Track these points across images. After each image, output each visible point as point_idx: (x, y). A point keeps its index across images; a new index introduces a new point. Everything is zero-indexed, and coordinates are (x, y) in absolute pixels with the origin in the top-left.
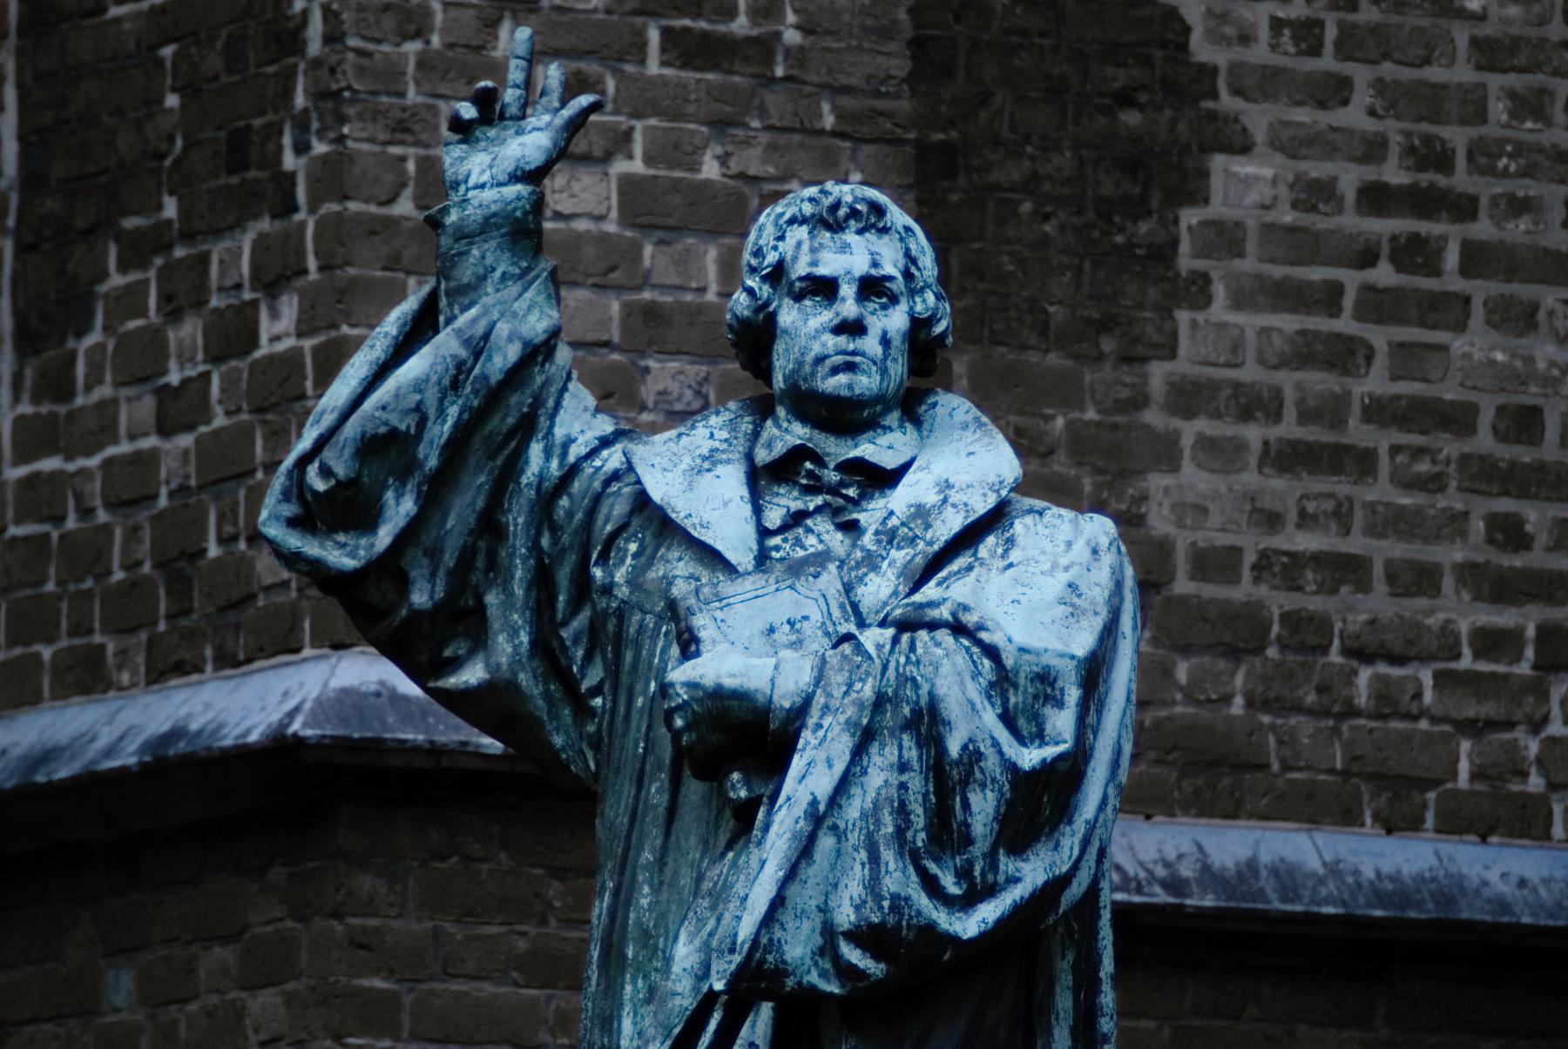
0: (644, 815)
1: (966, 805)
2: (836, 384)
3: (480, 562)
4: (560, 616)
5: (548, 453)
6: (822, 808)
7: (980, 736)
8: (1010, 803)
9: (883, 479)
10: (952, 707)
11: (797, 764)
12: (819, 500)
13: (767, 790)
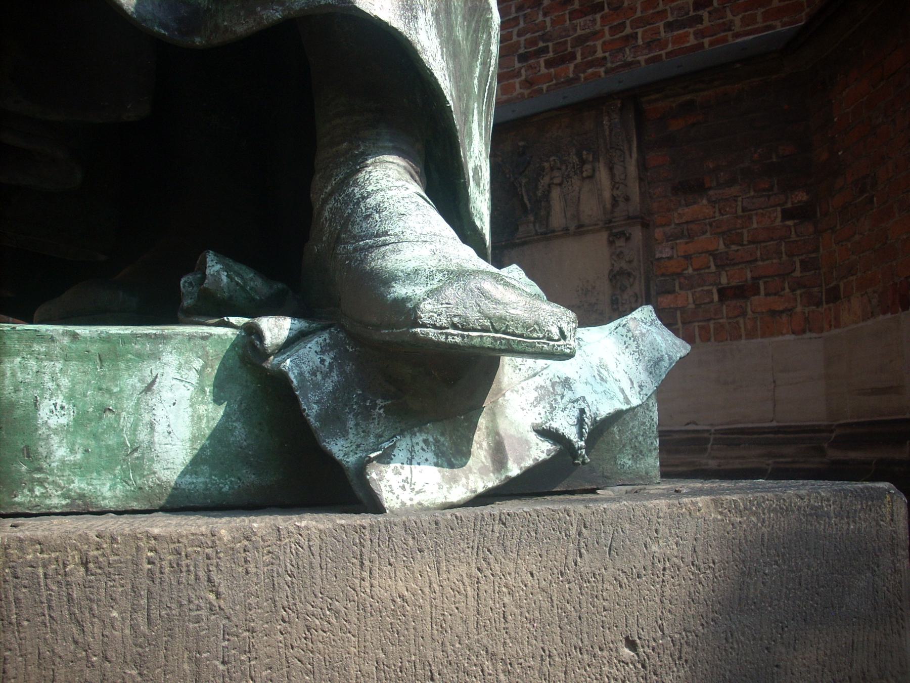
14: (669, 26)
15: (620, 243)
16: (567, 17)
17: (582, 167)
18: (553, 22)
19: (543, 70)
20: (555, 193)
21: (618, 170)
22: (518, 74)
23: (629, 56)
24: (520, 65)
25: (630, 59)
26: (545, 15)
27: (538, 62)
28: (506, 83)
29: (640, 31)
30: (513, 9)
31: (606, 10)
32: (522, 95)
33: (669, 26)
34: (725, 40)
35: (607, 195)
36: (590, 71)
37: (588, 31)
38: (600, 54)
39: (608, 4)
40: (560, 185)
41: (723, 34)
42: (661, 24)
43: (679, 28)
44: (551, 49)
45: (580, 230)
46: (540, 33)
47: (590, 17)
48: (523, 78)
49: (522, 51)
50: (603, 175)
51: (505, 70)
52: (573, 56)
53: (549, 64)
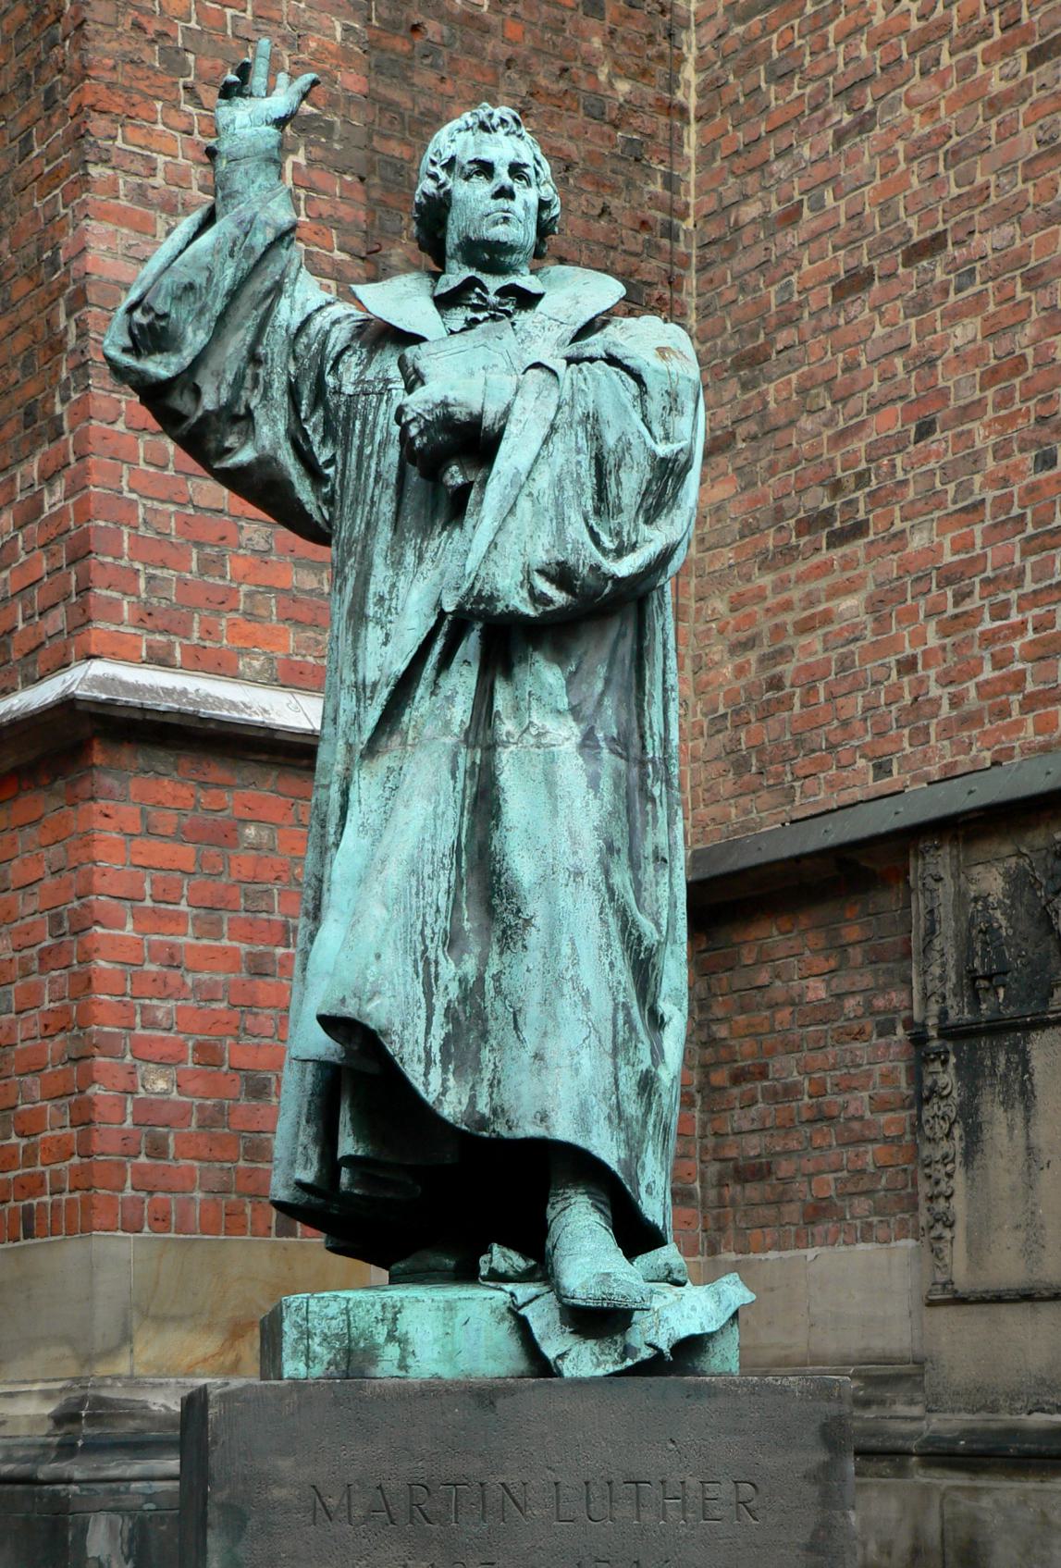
0: (377, 520)
1: (619, 483)
2: (500, 233)
3: (248, 383)
4: (303, 415)
5: (292, 309)
6: (523, 478)
7: (629, 429)
8: (650, 482)
9: (527, 300)
10: (607, 412)
11: (504, 448)
12: (486, 314)
13: (475, 476)
28: (1042, 711)
51: (1041, 687)
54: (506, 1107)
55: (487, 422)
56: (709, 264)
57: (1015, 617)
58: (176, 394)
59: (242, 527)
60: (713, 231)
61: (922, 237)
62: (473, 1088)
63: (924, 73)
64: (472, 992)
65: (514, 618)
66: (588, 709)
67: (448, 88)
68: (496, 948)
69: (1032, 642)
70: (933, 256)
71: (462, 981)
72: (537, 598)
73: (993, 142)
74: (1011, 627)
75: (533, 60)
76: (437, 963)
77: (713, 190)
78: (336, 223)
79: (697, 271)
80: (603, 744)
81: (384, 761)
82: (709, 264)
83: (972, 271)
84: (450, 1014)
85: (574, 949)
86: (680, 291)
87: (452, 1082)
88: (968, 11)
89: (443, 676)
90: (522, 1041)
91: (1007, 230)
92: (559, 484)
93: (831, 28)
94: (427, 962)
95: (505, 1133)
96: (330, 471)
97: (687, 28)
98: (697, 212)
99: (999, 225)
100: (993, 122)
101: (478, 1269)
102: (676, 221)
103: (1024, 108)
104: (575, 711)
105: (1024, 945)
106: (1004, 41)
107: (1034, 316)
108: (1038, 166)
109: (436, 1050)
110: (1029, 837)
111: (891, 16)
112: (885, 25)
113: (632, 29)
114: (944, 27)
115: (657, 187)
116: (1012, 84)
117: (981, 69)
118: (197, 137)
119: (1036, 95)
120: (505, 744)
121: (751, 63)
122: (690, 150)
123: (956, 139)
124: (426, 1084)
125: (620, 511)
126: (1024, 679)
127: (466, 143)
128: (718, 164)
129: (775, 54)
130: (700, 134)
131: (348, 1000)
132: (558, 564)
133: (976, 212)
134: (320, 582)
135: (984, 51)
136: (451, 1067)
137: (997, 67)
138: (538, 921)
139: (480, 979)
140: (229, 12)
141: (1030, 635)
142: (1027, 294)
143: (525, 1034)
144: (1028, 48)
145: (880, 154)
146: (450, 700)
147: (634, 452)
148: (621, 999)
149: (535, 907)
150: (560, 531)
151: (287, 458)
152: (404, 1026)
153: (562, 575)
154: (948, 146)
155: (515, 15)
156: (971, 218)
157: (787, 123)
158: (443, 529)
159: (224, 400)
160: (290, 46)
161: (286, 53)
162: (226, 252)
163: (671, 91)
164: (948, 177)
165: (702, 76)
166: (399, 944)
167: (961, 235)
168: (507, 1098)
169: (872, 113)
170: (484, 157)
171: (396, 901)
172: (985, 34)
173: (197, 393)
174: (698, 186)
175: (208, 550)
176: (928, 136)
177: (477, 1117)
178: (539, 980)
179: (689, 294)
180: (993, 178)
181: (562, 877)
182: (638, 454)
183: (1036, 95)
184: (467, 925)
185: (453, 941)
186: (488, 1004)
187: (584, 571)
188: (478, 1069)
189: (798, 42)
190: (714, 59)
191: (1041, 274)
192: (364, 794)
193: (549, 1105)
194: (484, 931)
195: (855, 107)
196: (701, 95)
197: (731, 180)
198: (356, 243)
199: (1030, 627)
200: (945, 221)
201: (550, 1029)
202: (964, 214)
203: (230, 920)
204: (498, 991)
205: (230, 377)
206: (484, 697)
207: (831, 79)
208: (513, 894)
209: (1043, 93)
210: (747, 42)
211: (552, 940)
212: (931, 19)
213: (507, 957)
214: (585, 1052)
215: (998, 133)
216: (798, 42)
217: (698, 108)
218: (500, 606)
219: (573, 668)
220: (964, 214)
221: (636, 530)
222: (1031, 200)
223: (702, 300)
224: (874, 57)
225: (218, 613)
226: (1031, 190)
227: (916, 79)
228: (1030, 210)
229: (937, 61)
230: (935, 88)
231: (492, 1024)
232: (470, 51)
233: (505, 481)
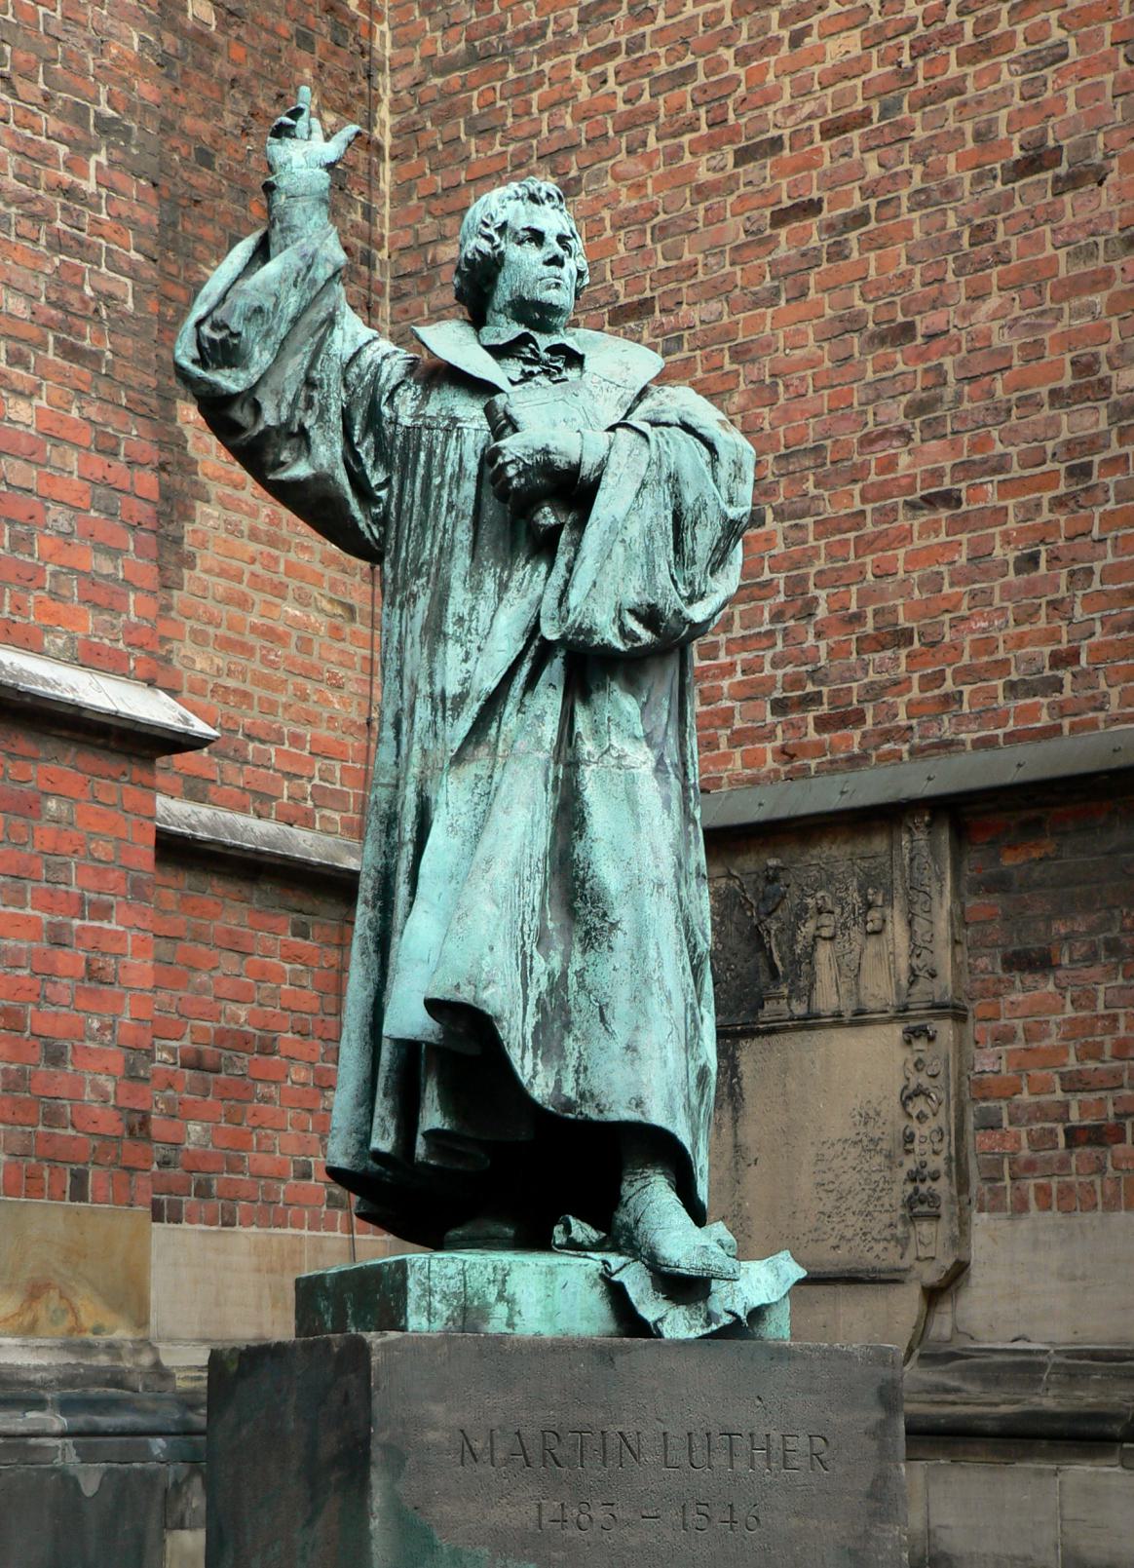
1: (694, 538)
4: (356, 440)
8: (719, 540)
10: (687, 474)
11: (601, 497)
14: (1012, 688)
15: (920, 1044)
16: (854, 647)
17: (866, 913)
18: (831, 651)
19: (812, 735)
20: (824, 952)
21: (921, 924)
22: (771, 736)
23: (946, 729)
24: (775, 719)
25: (948, 736)
26: (818, 635)
27: (804, 719)
28: (750, 747)
29: (967, 689)
30: (766, 615)
31: (916, 644)
32: (776, 771)
33: (1012, 688)
34: (1093, 725)
35: (903, 963)
36: (887, 747)
37: (886, 676)
38: (902, 720)
39: (921, 635)
40: (832, 938)
41: (1091, 715)
42: (999, 683)
43: (1027, 695)
44: (825, 700)
45: (860, 1018)
46: (809, 668)
47: (889, 653)
48: (779, 743)
49: (777, 694)
50: (897, 929)
51: (749, 725)
52: (859, 718)
53: (822, 724)
54: (596, 1092)
55: (585, 471)
56: (404, 295)
57: (723, 659)
58: (237, 407)
59: (48, 508)
60: (408, 264)
61: (629, 300)
62: (558, 1073)
63: (630, 152)
64: (558, 985)
65: (607, 650)
66: (658, 738)
67: (180, 98)
68: (578, 947)
69: (740, 683)
70: (639, 319)
71: (551, 975)
72: (625, 634)
73: (700, 224)
74: (719, 667)
75: (254, 83)
76: (532, 957)
77: (409, 226)
78: (133, 224)
79: (391, 300)
80: (670, 769)
81: (470, 770)
82: (404, 295)
83: (680, 338)
84: (540, 1006)
85: (659, 953)
86: (376, 317)
87: (540, 1067)
88: (675, 104)
89: (528, 696)
90: (612, 1034)
91: (715, 306)
92: (649, 534)
93: (535, 96)
94: (524, 955)
95: (594, 1115)
96: (383, 494)
97: (383, 71)
98: (391, 244)
99: (707, 301)
100: (701, 206)
101: (551, 1235)
102: (374, 251)
103: (731, 199)
104: (648, 738)
105: (733, 959)
106: (711, 137)
107: (742, 387)
108: (746, 252)
109: (529, 1036)
110: (740, 861)
111: (596, 95)
112: (590, 102)
113: (336, 65)
114: (651, 114)
115: (357, 217)
116: (719, 175)
117: (688, 158)
118: (12, 126)
119: (742, 190)
120: (588, 763)
121: (449, 114)
122: (386, 185)
123: (662, 217)
124: (522, 1068)
125: (694, 563)
126: (733, 717)
127: (517, 211)
128: (414, 202)
129: (476, 111)
130: (395, 172)
131: (462, 987)
132: (649, 606)
133: (684, 285)
134: (116, 568)
135: (691, 142)
136: (540, 1052)
137: (704, 158)
138: (624, 926)
139: (564, 974)
140: (41, 10)
141: (739, 677)
142: (735, 367)
143: (614, 1027)
144: (735, 147)
145: (585, 218)
146: (540, 718)
147: (709, 512)
148: (689, 1000)
149: (621, 912)
150: (651, 577)
151: (342, 477)
152: (511, 1013)
153: (650, 616)
154: (655, 221)
155: (238, 38)
156: (680, 289)
157: (488, 176)
158: (527, 562)
159: (284, 418)
160: (95, 50)
161: (91, 56)
162: (291, 281)
163: (369, 128)
164: (655, 250)
165: (398, 118)
166: (507, 938)
167: (669, 304)
168: (596, 1083)
169: (578, 180)
170: (536, 226)
171: (505, 899)
172: (692, 126)
173: (257, 409)
174: (391, 220)
175: (18, 528)
176: (636, 209)
177: (563, 1099)
178: (627, 978)
179: (384, 320)
180: (700, 257)
181: (648, 888)
182: (712, 513)
183: (742, 190)
184: (550, 925)
185: (542, 938)
186: (571, 997)
187: (669, 614)
188: (562, 1055)
189: (500, 104)
190: (409, 104)
191: (749, 350)
192: (452, 798)
193: (645, 1093)
194: (567, 931)
195: (561, 172)
196: (396, 135)
197: (428, 220)
198: (148, 244)
199: (739, 668)
200: (652, 289)
201: (641, 1023)
202: (672, 286)
203: (33, 889)
204: (582, 986)
205: (289, 397)
206: (568, 718)
207: (534, 142)
208: (599, 900)
209: (749, 188)
210: (445, 94)
211: (640, 943)
212: (638, 104)
213: (591, 956)
214: (669, 1046)
215: (706, 217)
216: (500, 104)
217: (392, 147)
218: (597, 639)
219: (644, 699)
220: (672, 286)
221: (706, 581)
222: (739, 282)
223: (396, 328)
224: (579, 129)
225: (27, 589)
226: (739, 273)
227: (623, 155)
228: (737, 291)
229: (644, 144)
230: (642, 167)
231: (575, 1015)
232: (200, 66)
233: (604, 527)
